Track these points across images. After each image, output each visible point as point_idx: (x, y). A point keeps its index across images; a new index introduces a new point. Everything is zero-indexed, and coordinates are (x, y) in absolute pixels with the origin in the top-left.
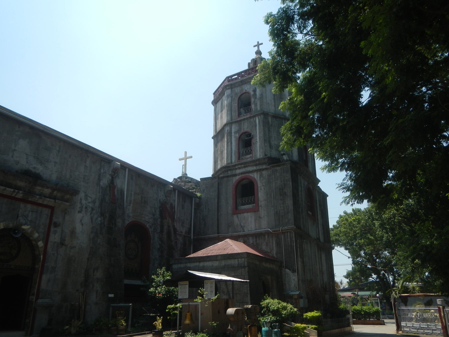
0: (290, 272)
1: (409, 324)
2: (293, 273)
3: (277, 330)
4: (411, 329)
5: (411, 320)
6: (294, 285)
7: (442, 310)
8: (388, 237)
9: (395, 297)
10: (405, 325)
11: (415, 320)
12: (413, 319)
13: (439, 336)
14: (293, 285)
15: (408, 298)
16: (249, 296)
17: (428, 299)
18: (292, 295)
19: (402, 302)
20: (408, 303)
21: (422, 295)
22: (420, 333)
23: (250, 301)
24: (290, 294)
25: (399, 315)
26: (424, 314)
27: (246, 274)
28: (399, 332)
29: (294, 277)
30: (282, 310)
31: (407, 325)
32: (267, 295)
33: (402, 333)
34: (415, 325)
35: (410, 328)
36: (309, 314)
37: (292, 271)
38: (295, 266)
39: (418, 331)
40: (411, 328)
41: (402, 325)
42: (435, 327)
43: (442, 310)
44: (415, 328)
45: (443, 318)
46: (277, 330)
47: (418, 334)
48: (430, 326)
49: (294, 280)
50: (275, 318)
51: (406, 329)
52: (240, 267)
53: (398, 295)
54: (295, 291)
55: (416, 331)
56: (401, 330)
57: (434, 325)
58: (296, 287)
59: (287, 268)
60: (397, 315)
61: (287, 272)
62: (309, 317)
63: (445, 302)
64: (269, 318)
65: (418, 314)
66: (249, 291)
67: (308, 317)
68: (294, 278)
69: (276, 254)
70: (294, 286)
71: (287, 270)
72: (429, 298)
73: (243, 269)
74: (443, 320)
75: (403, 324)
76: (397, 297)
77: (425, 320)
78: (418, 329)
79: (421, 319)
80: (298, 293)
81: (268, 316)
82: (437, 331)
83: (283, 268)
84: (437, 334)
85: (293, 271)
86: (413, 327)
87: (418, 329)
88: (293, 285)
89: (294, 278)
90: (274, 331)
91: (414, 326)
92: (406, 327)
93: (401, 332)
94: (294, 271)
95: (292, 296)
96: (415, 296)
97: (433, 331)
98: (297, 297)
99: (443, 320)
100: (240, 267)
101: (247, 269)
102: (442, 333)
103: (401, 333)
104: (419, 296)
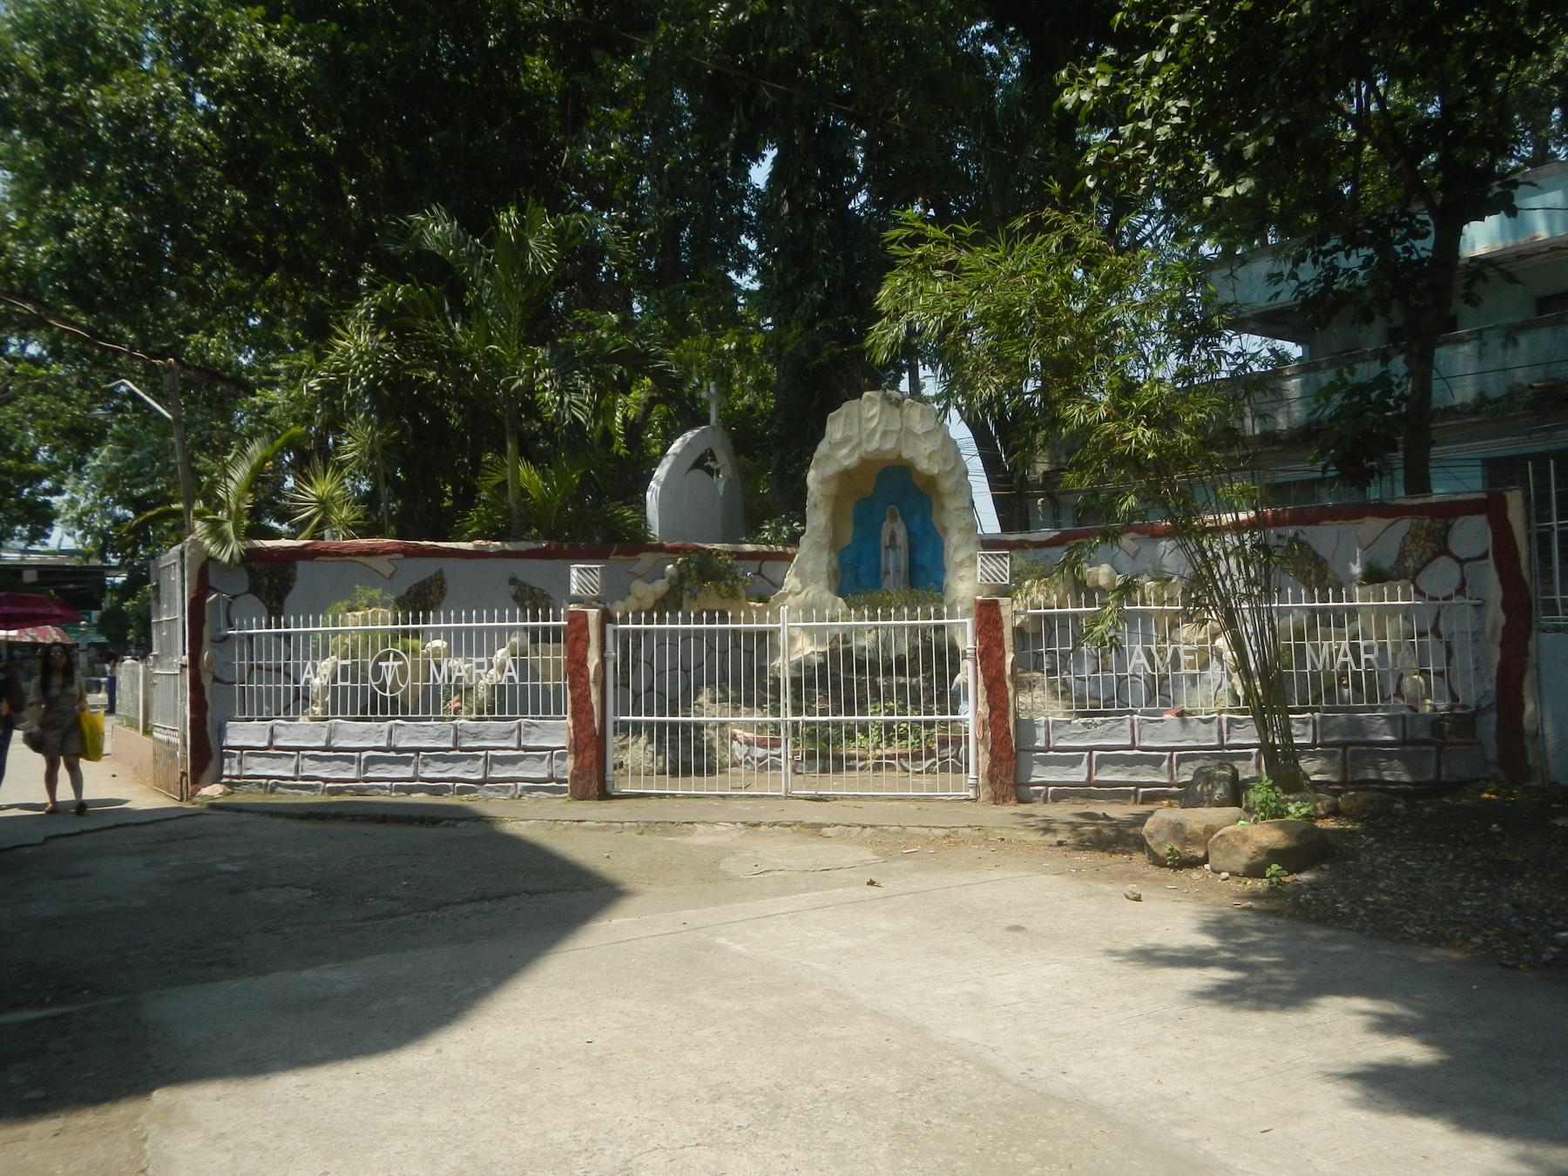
1: (302, 731)
4: (307, 762)
5: (300, 699)
7: (593, 633)
8: (101, 224)
9: (211, 560)
10: (265, 744)
11: (325, 704)
12: (306, 698)
13: (535, 794)
15: (302, 567)
17: (422, 570)
19: (254, 589)
20: (290, 601)
21: (392, 548)
22: (387, 784)
25: (216, 679)
26: (439, 667)
28: (205, 791)
31: (278, 742)
33: (225, 794)
34: (350, 736)
35: (304, 757)
39: (368, 775)
40: (312, 757)
41: (230, 742)
42: (515, 745)
43: (593, 633)
44: (346, 755)
45: (595, 682)
47: (360, 792)
48: (476, 736)
51: (258, 767)
53: (235, 546)
55: (351, 775)
56: (218, 779)
57: (513, 731)
60: (207, 681)
63: (513, 589)
65: (383, 664)
72: (425, 568)
74: (595, 697)
75: (240, 734)
76: (226, 558)
77: (376, 707)
78: (372, 761)
79: (405, 695)
82: (520, 764)
84: (520, 785)
86: (329, 752)
87: (372, 761)
91: (401, 744)
92: (271, 751)
93: (212, 791)
96: (349, 554)
97: (496, 766)
99: (595, 697)
102: (567, 777)
103: (216, 794)
104: (372, 552)
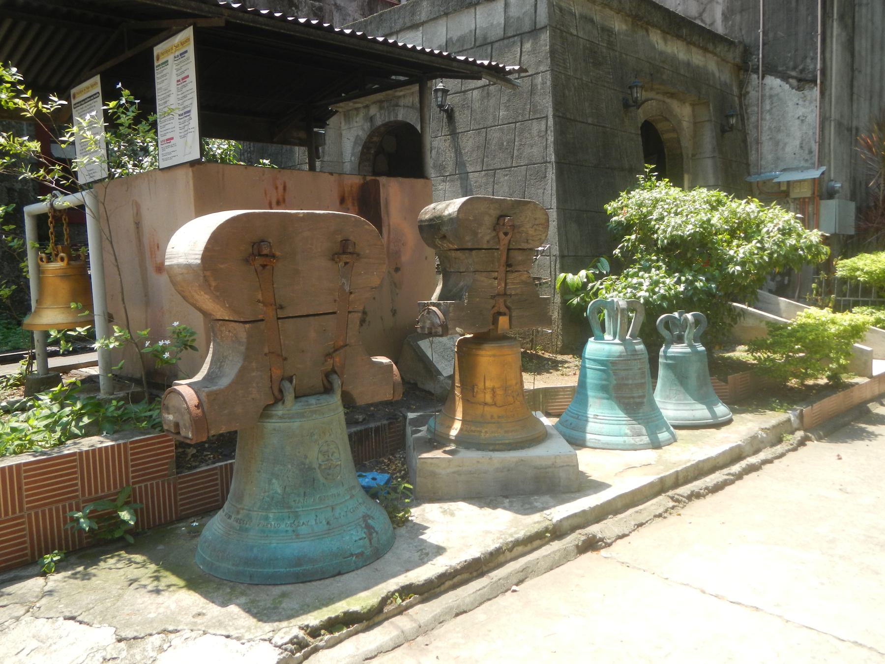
0: (787, 87)
2: (799, 89)
3: (689, 350)
6: (801, 144)
14: (792, 145)
16: (551, 175)
18: (788, 182)
23: (554, 200)
24: (776, 180)
27: (542, 68)
29: (804, 106)
30: (729, 243)
32: (652, 171)
36: (869, 261)
37: (794, 82)
38: (814, 59)
46: (689, 350)
49: (802, 120)
50: (679, 282)
52: (514, 36)
54: (803, 169)
58: (810, 152)
59: (771, 69)
61: (771, 89)
62: (867, 273)
64: (641, 284)
66: (551, 149)
67: (858, 273)
68: (801, 114)
69: (726, 17)
70: (801, 147)
71: (773, 82)
73: (528, 46)
80: (816, 174)
81: (640, 270)
83: (754, 76)
85: (799, 80)
88: (798, 142)
89: (801, 111)
90: (666, 357)
94: (804, 81)
95: (784, 188)
98: (808, 194)
100: (514, 36)
101: (545, 38)
